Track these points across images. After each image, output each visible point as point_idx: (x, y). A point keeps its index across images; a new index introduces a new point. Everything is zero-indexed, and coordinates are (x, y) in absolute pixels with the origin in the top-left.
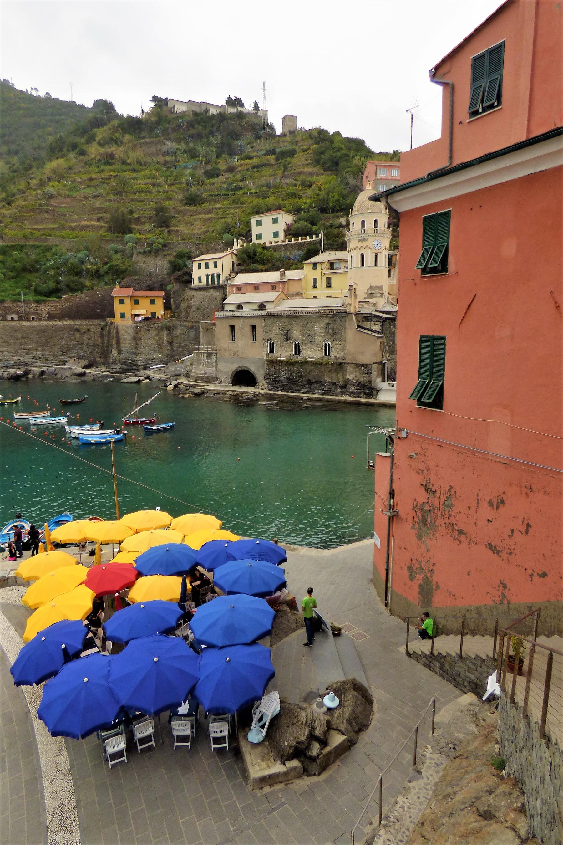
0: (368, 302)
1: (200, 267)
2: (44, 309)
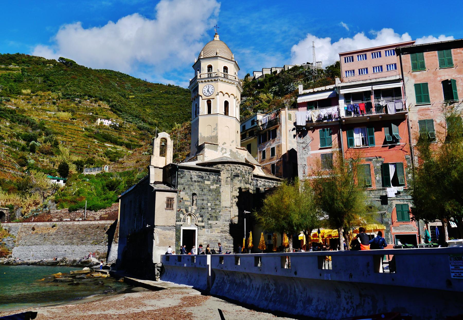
2: (100, 213)
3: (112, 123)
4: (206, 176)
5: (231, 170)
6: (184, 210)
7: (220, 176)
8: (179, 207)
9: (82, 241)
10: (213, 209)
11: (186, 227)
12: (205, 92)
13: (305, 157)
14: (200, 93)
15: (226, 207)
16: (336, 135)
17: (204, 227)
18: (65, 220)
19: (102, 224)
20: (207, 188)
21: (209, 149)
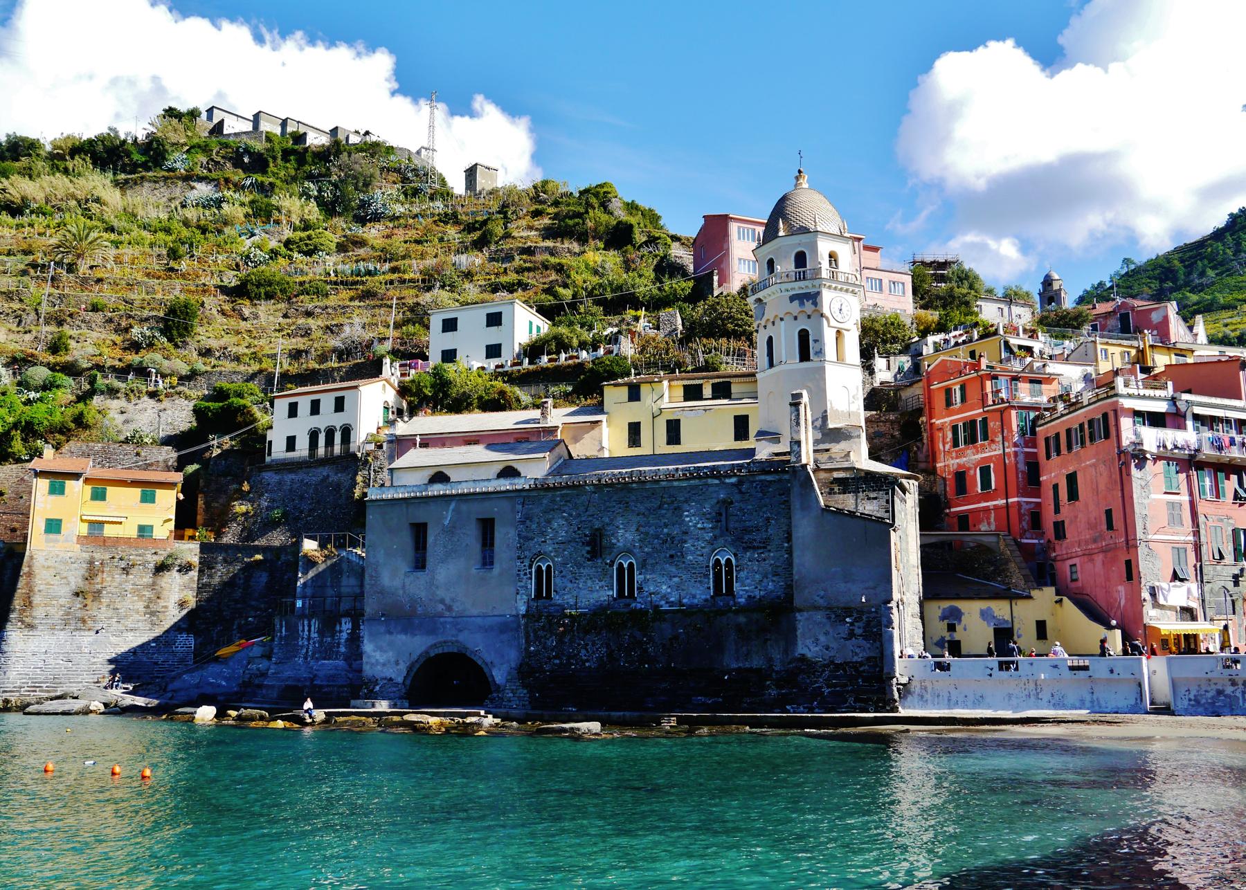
0: (827, 450)
1: (293, 411)
13: (1146, 501)
16: (1184, 475)
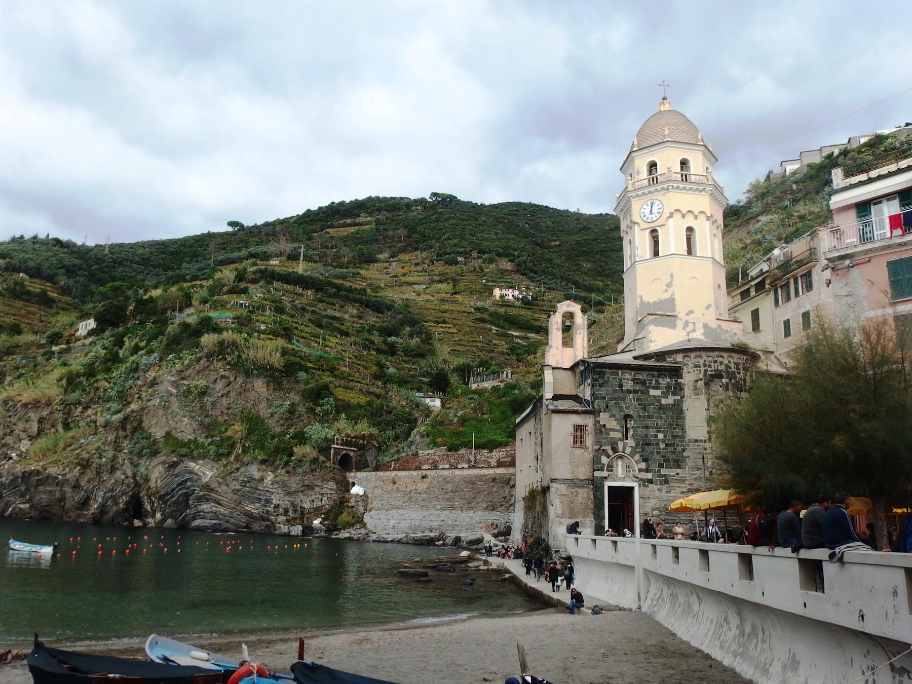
3: (520, 294)
4: (652, 380)
5: (705, 365)
6: (608, 448)
7: (682, 378)
8: (599, 443)
9: (469, 504)
10: (670, 445)
11: (614, 480)
12: (645, 216)
14: (636, 217)
15: (696, 441)
17: (650, 481)
18: (441, 467)
19: (501, 475)
20: (654, 404)
21: (657, 326)
